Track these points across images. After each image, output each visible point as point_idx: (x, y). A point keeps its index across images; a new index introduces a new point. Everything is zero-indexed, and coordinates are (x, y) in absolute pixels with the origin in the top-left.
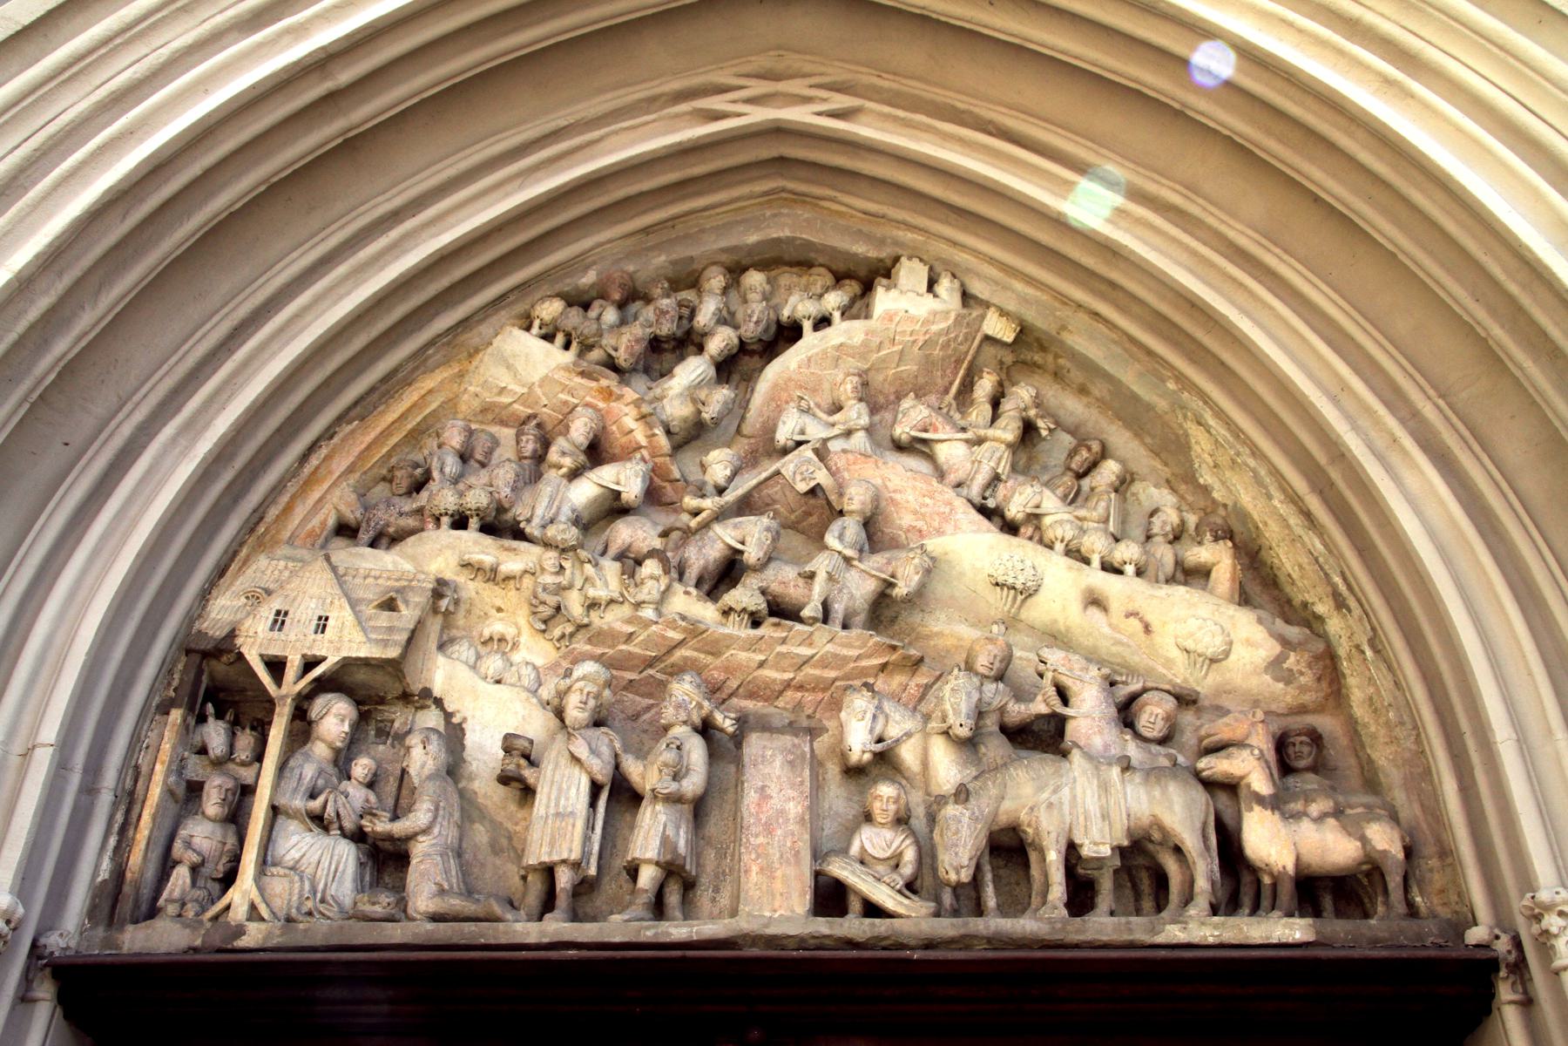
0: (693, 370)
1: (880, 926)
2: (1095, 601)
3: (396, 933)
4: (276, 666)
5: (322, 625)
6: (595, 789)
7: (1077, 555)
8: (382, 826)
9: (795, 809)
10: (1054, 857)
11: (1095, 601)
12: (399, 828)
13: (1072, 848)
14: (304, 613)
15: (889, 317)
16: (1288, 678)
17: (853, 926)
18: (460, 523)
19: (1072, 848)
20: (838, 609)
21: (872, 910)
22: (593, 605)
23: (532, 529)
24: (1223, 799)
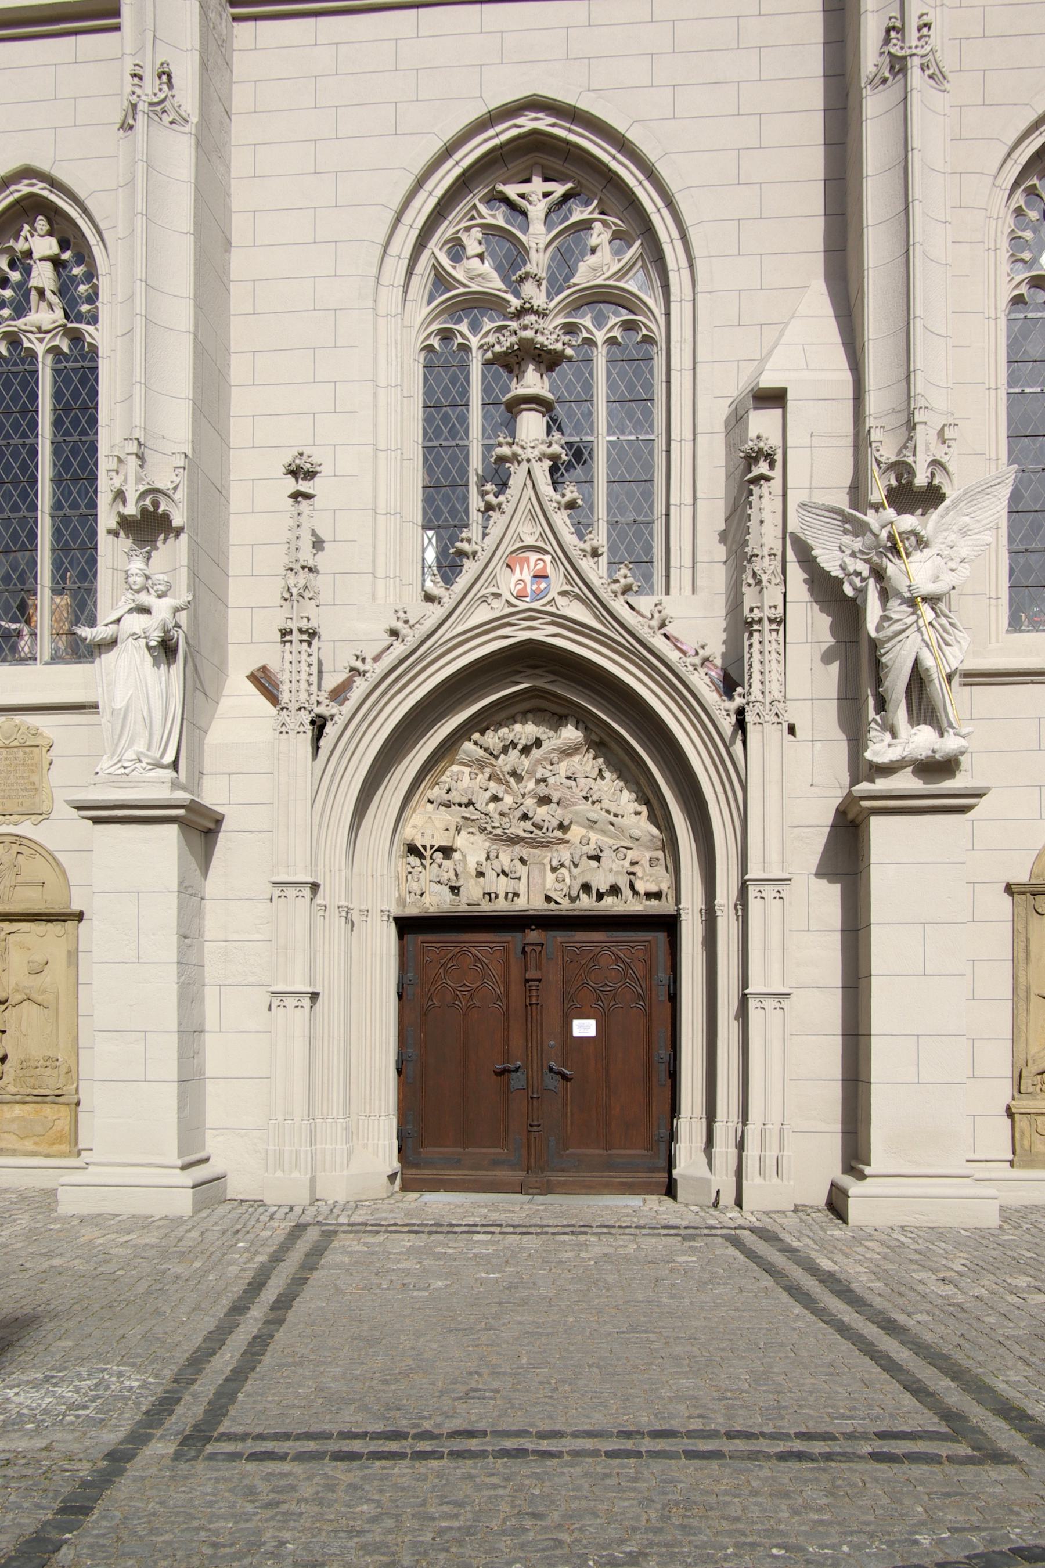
0: (514, 754)
1: (558, 906)
2: (612, 824)
3: (460, 909)
4: (424, 847)
5: (433, 836)
6: (498, 875)
7: (608, 812)
8: (453, 884)
9: (540, 881)
10: (594, 892)
11: (612, 824)
12: (457, 885)
13: (598, 890)
14: (428, 833)
15: (565, 739)
16: (654, 843)
17: (552, 906)
18: (460, 805)
19: (598, 890)
20: (550, 829)
21: (557, 903)
22: (494, 828)
23: (478, 806)
24: (632, 877)
